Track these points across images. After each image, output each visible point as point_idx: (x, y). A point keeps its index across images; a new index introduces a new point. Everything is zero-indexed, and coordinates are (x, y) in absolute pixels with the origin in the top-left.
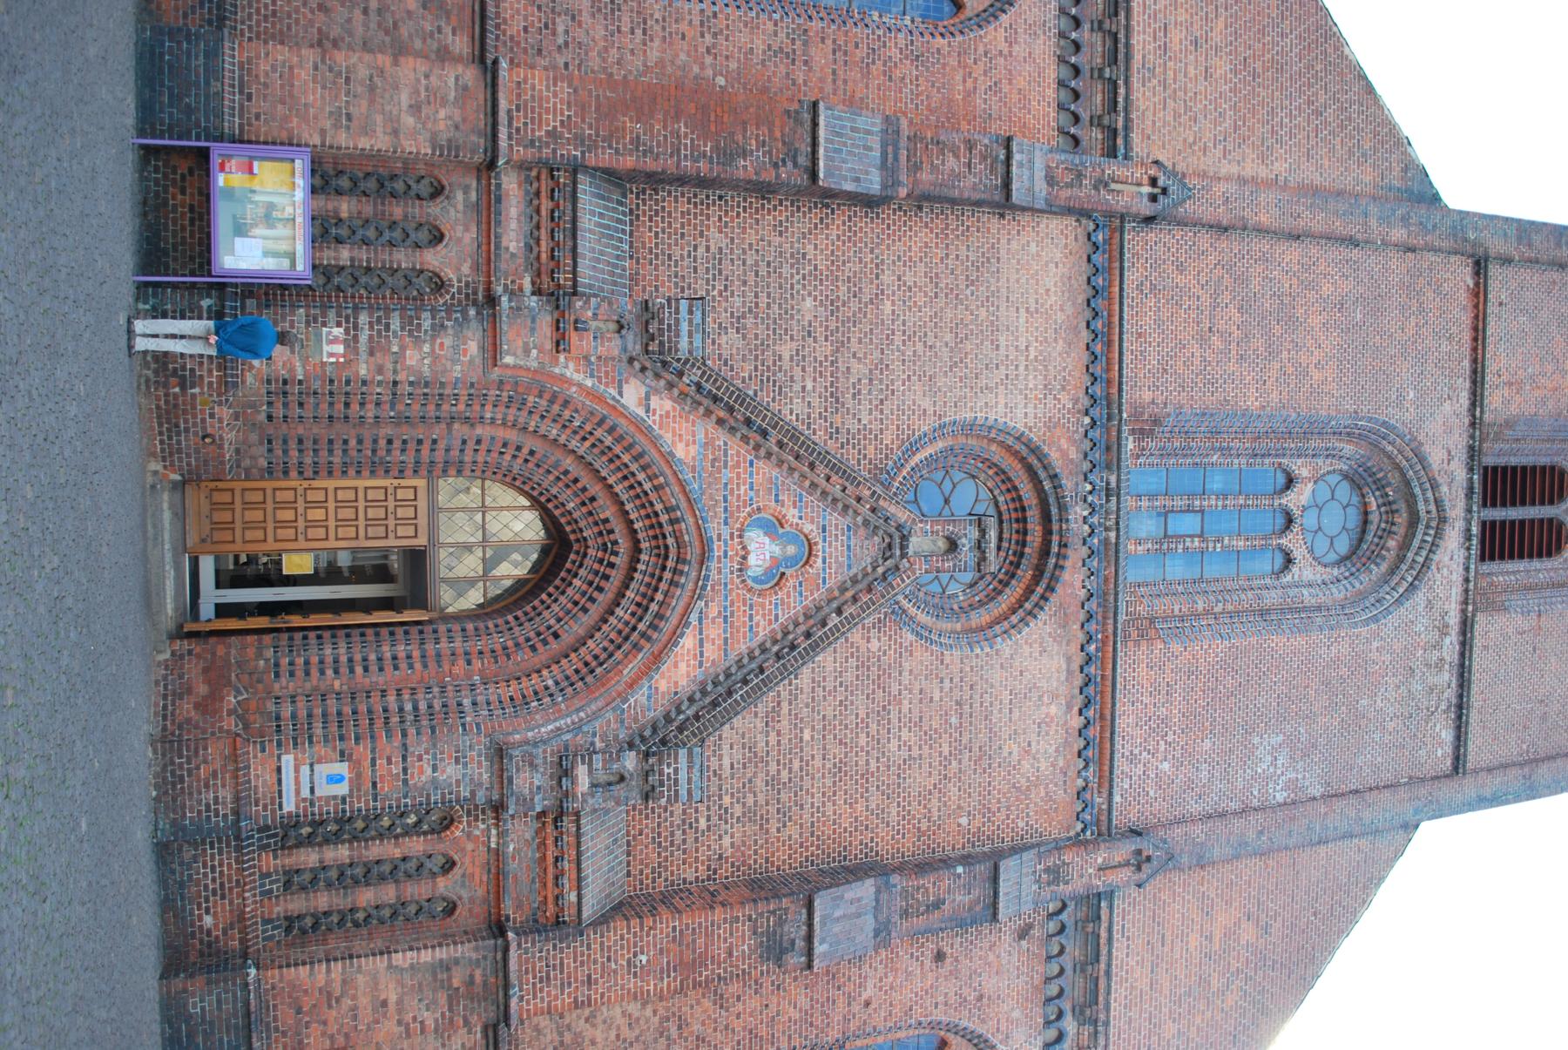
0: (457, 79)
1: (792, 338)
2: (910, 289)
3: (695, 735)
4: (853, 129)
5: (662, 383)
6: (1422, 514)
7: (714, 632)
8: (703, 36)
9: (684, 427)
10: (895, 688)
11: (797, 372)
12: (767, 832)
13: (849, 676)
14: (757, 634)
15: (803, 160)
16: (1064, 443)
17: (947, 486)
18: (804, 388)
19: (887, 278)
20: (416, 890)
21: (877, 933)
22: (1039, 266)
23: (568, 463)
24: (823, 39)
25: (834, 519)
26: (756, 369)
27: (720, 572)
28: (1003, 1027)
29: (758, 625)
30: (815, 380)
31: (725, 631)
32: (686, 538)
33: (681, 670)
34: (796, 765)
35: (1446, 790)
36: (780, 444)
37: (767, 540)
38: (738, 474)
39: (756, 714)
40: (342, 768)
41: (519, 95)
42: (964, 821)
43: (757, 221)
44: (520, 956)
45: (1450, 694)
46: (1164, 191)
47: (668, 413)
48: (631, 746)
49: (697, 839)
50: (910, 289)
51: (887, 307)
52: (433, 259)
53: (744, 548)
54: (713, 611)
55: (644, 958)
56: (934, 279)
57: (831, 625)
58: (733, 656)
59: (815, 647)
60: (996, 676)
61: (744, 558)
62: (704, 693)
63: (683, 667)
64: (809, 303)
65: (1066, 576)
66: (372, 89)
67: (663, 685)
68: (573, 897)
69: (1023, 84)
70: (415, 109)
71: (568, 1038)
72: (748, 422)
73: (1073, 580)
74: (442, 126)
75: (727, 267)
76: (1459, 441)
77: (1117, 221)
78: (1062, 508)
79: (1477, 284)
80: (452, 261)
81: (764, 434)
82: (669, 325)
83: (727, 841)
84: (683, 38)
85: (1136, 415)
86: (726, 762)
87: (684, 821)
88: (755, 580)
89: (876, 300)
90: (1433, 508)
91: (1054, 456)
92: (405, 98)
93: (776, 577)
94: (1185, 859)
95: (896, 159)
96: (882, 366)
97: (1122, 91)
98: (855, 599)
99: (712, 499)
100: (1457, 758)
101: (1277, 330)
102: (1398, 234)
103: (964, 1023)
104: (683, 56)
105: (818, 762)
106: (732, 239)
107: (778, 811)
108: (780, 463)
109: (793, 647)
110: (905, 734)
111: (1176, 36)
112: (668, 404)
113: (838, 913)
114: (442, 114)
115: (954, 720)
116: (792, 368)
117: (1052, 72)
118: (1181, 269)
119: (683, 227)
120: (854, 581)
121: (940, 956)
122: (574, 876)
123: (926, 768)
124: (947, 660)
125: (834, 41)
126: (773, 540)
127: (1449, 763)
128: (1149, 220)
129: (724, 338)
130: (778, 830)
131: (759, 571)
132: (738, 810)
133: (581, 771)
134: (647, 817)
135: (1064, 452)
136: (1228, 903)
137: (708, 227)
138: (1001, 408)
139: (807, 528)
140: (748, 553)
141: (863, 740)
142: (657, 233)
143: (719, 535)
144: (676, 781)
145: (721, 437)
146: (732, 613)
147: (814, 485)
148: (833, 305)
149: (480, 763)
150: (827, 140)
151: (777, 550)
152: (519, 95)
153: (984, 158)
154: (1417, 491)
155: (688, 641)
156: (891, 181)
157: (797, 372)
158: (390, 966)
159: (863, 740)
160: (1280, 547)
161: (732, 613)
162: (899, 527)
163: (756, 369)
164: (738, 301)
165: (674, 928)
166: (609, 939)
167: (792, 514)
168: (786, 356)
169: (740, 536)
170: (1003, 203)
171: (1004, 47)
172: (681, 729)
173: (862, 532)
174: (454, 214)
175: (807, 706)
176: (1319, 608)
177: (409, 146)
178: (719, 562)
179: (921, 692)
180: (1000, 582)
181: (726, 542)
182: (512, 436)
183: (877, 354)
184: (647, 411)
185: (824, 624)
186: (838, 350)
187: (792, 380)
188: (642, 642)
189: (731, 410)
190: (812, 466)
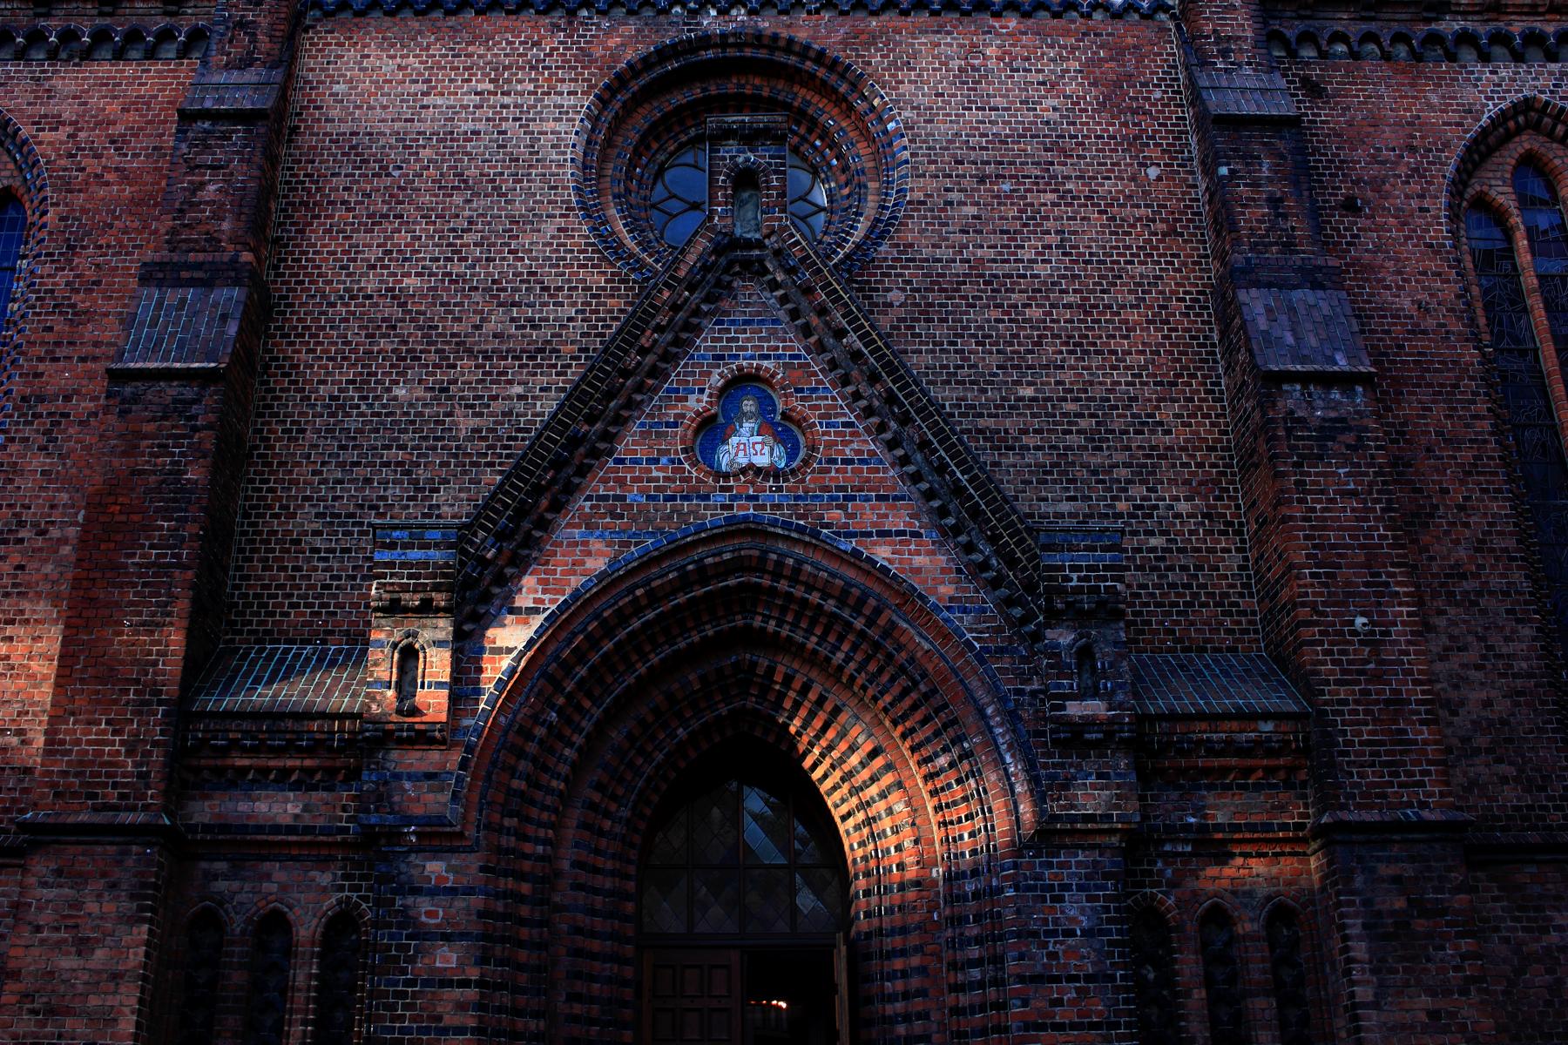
0: (44, 885)
1: (450, 414)
2: (387, 252)
3: (1022, 541)
4: (154, 324)
5: (496, 590)
7: (868, 515)
8: (21, 541)
9: (560, 562)
10: (959, 268)
11: (498, 406)
12: (1170, 448)
14: (872, 453)
15: (189, 393)
16: (614, 42)
17: (674, 206)
18: (520, 397)
19: (371, 284)
20: (1257, 968)
21: (1316, 286)
23: (616, 736)
24: (38, 375)
25: (703, 344)
26: (491, 464)
27: (779, 507)
28: (1456, 117)
29: (858, 452)
30: (510, 382)
31: (867, 499)
32: (727, 556)
34: (1070, 407)
36: (591, 419)
37: (734, 440)
38: (634, 480)
39: (995, 464)
41: (75, 795)
42: (1153, 172)
43: (281, 464)
44: (1359, 806)
47: (540, 581)
48: (1037, 636)
49: (1179, 550)
50: (387, 252)
51: (411, 282)
52: (307, 928)
53: (744, 471)
54: (836, 515)
55: (1360, 620)
56: (377, 219)
57: (859, 344)
58: (903, 488)
59: (891, 369)
61: (758, 471)
62: (957, 530)
63: (919, 560)
64: (400, 392)
65: (802, 36)
66: (51, 1011)
67: (946, 590)
68: (1268, 727)
69: (116, 106)
70: (83, 946)
71: (1481, 741)
72: (558, 464)
74: (109, 907)
75: (345, 506)
78: (705, 41)
80: (311, 899)
81: (575, 441)
82: (410, 576)
83: (1183, 507)
84: (21, 567)
86: (1065, 507)
87: (1153, 569)
88: (791, 456)
89: (398, 297)
92: (67, 962)
95: (199, 266)
96: (494, 290)
98: (822, 311)
99: (670, 517)
103: (1450, 170)
104: (48, 568)
105: (1068, 376)
106: (306, 499)
107: (1137, 432)
108: (620, 421)
109: (891, 399)
110: (1027, 254)
112: (528, 581)
113: (1290, 339)
114: (92, 907)
115: (1006, 187)
116: (491, 415)
117: (104, 69)
119: (285, 569)
120: (794, 314)
121: (1350, 206)
122: (1235, 725)
123: (1075, 225)
124: (920, 196)
125: (41, 360)
126: (735, 432)
129: (445, 509)
130: (1168, 432)
131: (779, 450)
132: (1138, 491)
133: (1074, 709)
134: (1149, 623)
137: (287, 532)
138: (561, 127)
139: (716, 380)
140: (751, 466)
141: (1035, 313)
142: (292, 605)
143: (724, 507)
144: (1089, 568)
146: (839, 489)
147: (654, 372)
148: (405, 358)
149: (1061, 865)
150: (165, 359)
151: (747, 425)
152: (75, 795)
155: (882, 553)
156: (229, 273)
157: (498, 406)
158: (1376, 1005)
159: (1035, 313)
161: (839, 489)
163: (491, 464)
164: (393, 491)
165: (1313, 575)
166: (1332, 672)
167: (697, 403)
168: (474, 422)
169: (726, 476)
171: (62, 134)
172: (1012, 562)
173: (725, 305)
174: (242, 894)
175: (984, 391)
177: (136, 956)
178: (763, 507)
179: (963, 232)
180: (810, 131)
181: (733, 498)
182: (575, 815)
183: (477, 297)
184: (536, 611)
185: (856, 356)
186: (470, 351)
187: (510, 413)
188: (882, 621)
189: (538, 490)
190: (626, 374)
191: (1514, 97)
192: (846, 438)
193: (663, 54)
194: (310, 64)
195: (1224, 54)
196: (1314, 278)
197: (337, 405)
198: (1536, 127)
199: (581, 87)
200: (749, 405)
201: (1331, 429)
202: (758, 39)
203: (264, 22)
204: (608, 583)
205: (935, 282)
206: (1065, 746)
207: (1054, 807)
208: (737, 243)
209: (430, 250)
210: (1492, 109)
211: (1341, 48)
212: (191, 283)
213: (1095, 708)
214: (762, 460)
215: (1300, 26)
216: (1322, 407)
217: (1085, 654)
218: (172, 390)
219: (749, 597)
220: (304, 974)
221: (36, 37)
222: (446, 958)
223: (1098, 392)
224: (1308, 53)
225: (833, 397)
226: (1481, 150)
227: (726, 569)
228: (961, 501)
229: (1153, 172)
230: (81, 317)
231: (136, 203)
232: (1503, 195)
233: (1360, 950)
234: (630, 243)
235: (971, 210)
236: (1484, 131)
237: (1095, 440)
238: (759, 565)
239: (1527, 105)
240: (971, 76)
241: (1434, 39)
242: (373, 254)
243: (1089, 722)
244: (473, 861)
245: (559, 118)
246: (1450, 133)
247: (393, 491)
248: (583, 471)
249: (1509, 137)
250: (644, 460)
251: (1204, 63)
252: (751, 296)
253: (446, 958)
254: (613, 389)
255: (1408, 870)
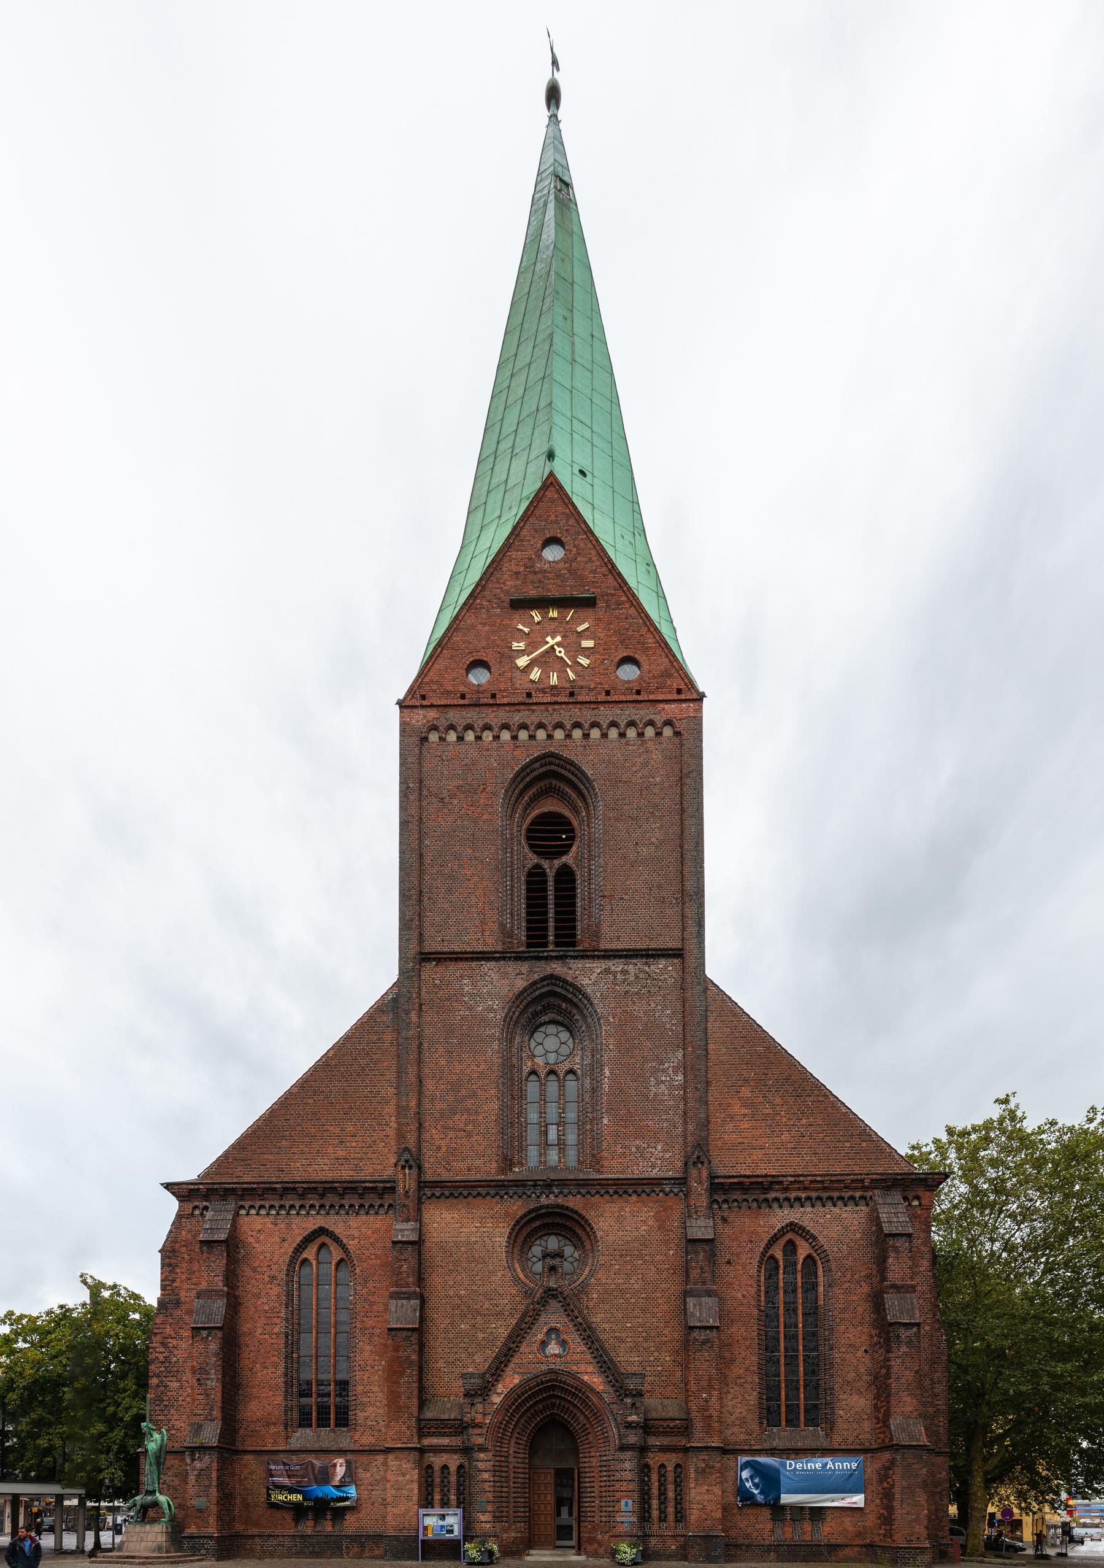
6: (549, 988)
7: (583, 1368)
9: (508, 1380)
10: (613, 1286)
11: (489, 1331)
13: (607, 1307)
15: (409, 1334)
17: (535, 1259)
19: (451, 1293)
20: (671, 1477)
22: (444, 1222)
23: (523, 1421)
25: (542, 1319)
28: (766, 1229)
33: (595, 1380)
35: (691, 961)
40: (623, 1502)
42: (671, 1252)
45: (640, 963)
46: (407, 1161)
52: (453, 1468)
59: (590, 1328)
60: (611, 1238)
61: (555, 1355)
65: (571, 1205)
67: (601, 1387)
69: (370, 1232)
70: (404, 1475)
72: (505, 1356)
73: (574, 1202)
76: (511, 967)
77: (422, 1185)
78: (542, 1207)
79: (434, 959)
80: (453, 1461)
81: (510, 1349)
83: (668, 1358)
85: (502, 1171)
89: (460, 1297)
90: (545, 983)
91: (521, 1213)
92: (401, 1478)
93: (563, 1343)
94: (703, 1134)
96: (485, 1295)
97: (367, 1185)
100: (675, 956)
101: (464, 1092)
102: (413, 1016)
103: (761, 1249)
105: (640, 1320)
108: (520, 1342)
111: (341, 1153)
112: (500, 1386)
117: (363, 1218)
118: (439, 1148)
121: (729, 1262)
127: (676, 961)
128: (420, 1168)
132: (656, 1354)
133: (630, 1419)
135: (518, 1207)
136: (729, 1105)
138: (501, 1239)
139: (545, 1330)
141: (633, 1300)
145: (512, 1365)
147: (529, 1328)
148: (463, 1316)
153: (402, 1254)
154: (537, 993)
155: (586, 1378)
157: (489, 1331)
159: (633, 1300)
160: (564, 1077)
162: (545, 1292)
164: (463, 1355)
167: (540, 1337)
170: (418, 1244)
174: (437, 1461)
176: (593, 1056)
177: (416, 1477)
182: (513, 1440)
191: (787, 1221)
192: (577, 1345)
193: (529, 1212)
194: (426, 1216)
195: (696, 1212)
196: (709, 1294)
197: (446, 1331)
198: (793, 1230)
199: (506, 1225)
200: (553, 1336)
201: (704, 1342)
202: (558, 1206)
203: (411, 1205)
204: (519, 1386)
205: (606, 1292)
206: (626, 1427)
207: (624, 1442)
208: (550, 1289)
209: (466, 1282)
210: (779, 1226)
211: (736, 1204)
212: (404, 1298)
213: (634, 1418)
214: (557, 1352)
215: (724, 1197)
216: (702, 1336)
217: (633, 1404)
218: (405, 1334)
219: (554, 1387)
220: (453, 1478)
221: (342, 1206)
222: (486, 1476)
223: (648, 1325)
224: (725, 1206)
225: (576, 1335)
226: (774, 1240)
227: (547, 1381)
228: (607, 1366)
229: (671, 1252)
230: (372, 1304)
231: (381, 1265)
232: (779, 1255)
233: (693, 1475)
234: (521, 1276)
235: (617, 1267)
236: (775, 1234)
237: (646, 1340)
238: (556, 1380)
239: (791, 1223)
240: (620, 1219)
241: (766, 1200)
242: (451, 1283)
243: (633, 1422)
244: (490, 1454)
245: (500, 1236)
246: (764, 1235)
247: (463, 1355)
248: (512, 1356)
249: (784, 1234)
250: (527, 1352)
251: (690, 1216)
252: (554, 1304)
253: (486, 1476)
254: (517, 1336)
255: (706, 1457)
